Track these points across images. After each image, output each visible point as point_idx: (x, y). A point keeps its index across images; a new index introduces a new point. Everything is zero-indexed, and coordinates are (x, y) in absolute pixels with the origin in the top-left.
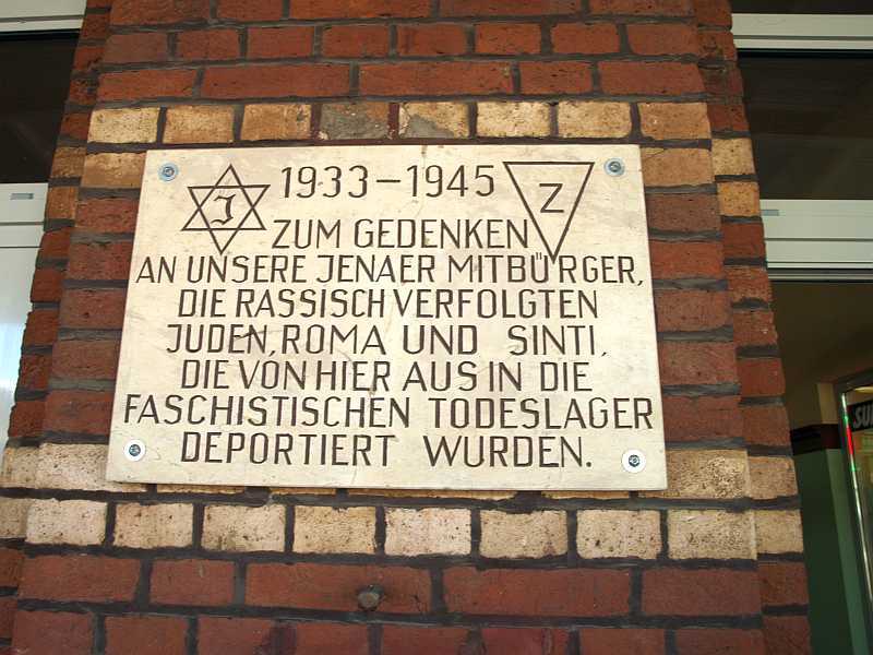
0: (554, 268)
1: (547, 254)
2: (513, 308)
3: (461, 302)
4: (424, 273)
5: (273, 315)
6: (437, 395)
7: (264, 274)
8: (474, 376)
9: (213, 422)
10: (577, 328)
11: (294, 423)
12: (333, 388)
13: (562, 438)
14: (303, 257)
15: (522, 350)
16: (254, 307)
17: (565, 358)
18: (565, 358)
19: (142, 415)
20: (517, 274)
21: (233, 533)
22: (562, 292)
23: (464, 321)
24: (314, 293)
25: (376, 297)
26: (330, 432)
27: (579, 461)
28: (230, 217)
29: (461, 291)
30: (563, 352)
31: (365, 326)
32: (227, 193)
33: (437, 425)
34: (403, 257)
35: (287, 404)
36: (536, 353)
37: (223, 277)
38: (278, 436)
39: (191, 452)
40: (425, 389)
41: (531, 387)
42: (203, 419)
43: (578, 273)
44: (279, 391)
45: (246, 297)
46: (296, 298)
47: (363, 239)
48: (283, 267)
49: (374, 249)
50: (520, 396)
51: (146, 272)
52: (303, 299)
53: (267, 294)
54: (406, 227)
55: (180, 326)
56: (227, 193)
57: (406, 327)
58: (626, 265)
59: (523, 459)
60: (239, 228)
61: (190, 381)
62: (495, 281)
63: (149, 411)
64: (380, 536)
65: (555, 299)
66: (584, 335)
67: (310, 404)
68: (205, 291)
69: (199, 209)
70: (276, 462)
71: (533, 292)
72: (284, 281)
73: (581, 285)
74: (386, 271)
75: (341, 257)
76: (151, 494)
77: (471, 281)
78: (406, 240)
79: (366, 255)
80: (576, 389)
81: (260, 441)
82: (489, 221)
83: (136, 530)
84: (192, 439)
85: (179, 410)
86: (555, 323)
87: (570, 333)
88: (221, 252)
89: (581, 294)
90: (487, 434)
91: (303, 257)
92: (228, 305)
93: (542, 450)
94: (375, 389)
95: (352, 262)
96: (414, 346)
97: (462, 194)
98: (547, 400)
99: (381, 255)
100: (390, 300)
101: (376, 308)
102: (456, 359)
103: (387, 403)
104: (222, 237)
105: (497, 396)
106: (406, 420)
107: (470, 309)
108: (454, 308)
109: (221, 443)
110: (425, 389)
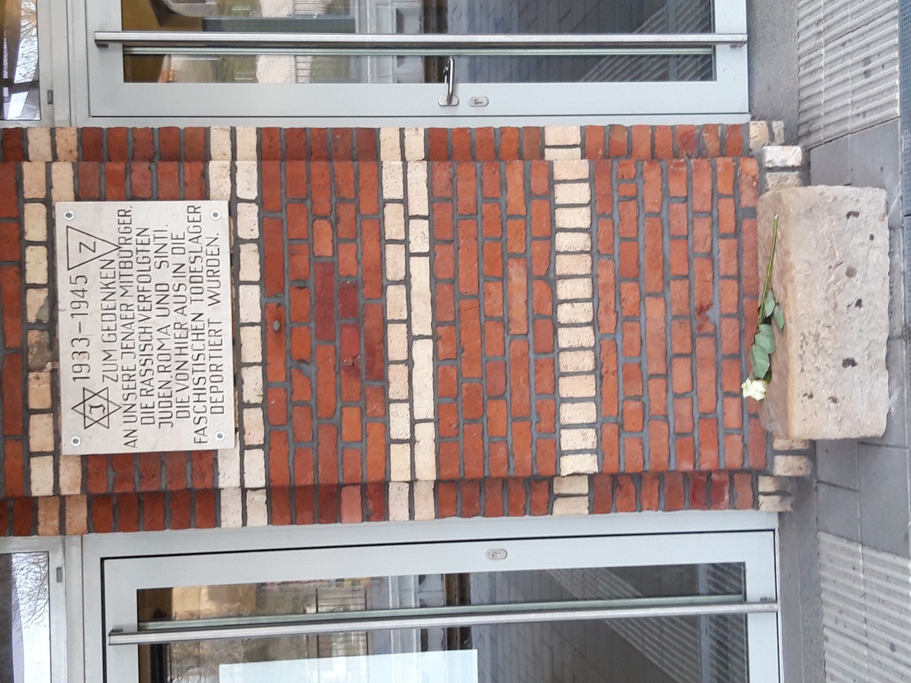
2: (146, 267)
6: (189, 301)
21: (255, 390)
23: (153, 290)
25: (142, 330)
32: (88, 408)
35: (196, 368)
39: (220, 410)
41: (183, 259)
43: (127, 236)
44: (189, 372)
45: (144, 392)
46: (144, 368)
47: (112, 338)
50: (188, 264)
51: (132, 444)
54: (105, 318)
56: (88, 408)
58: (122, 213)
59: (216, 263)
63: (201, 432)
64: (252, 324)
65: (140, 247)
66: (158, 234)
67: (195, 358)
74: (129, 326)
76: (240, 429)
81: (213, 379)
83: (256, 433)
84: (214, 410)
86: (153, 248)
90: (205, 278)
92: (148, 401)
95: (125, 343)
96: (165, 312)
99: (120, 329)
100: (142, 324)
101: (147, 330)
102: (172, 293)
104: (112, 408)
105: (189, 275)
107: (147, 286)
108: (146, 294)
109: (215, 396)
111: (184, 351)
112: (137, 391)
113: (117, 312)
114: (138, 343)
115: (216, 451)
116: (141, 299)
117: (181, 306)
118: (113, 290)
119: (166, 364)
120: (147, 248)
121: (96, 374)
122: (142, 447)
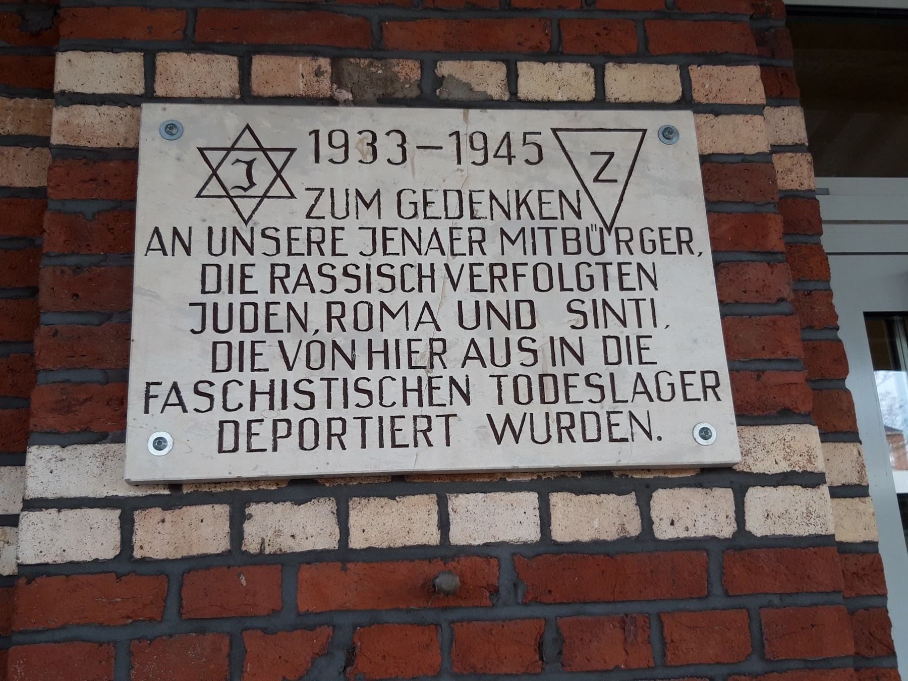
0: (610, 241)
1: (602, 226)
2: (570, 282)
3: (516, 276)
4: (476, 246)
5: (313, 291)
7: (300, 246)
8: (534, 352)
9: (253, 408)
10: (637, 301)
11: (346, 406)
12: (387, 367)
13: (630, 412)
14: (342, 229)
15: (582, 324)
16: (290, 283)
17: (626, 332)
18: (626, 332)
19: (166, 404)
20: (572, 246)
21: (278, 533)
22: (620, 265)
23: (519, 296)
24: (357, 267)
25: (426, 271)
26: (387, 414)
27: (649, 435)
28: (252, 184)
29: (515, 266)
30: (625, 326)
31: (416, 302)
32: (248, 156)
33: (500, 402)
34: (451, 229)
35: (337, 386)
36: (597, 326)
37: (251, 251)
38: (329, 420)
39: (229, 444)
40: (484, 365)
41: (594, 361)
42: (241, 405)
43: (635, 245)
44: (327, 372)
45: (280, 272)
46: (338, 273)
47: (408, 210)
48: (320, 240)
49: (420, 221)
50: (584, 371)
51: (156, 244)
52: (346, 273)
53: (304, 269)
54: (453, 198)
55: (204, 305)
56: (248, 156)
57: (460, 303)
58: (685, 236)
59: (592, 434)
60: (265, 196)
61: (222, 363)
62: (549, 253)
63: (174, 399)
64: (444, 525)
65: (613, 271)
66: (645, 307)
67: (362, 385)
68: (231, 266)
69: (215, 173)
70: (329, 448)
71: (589, 265)
72: (322, 253)
73: (638, 257)
74: (435, 244)
75: (385, 229)
76: (177, 494)
77: (525, 253)
78: (454, 211)
79: (411, 227)
80: (641, 362)
81: (309, 427)
82: (540, 192)
83: (158, 538)
84: (229, 428)
85: (211, 397)
86: (614, 296)
87: (631, 307)
88: (246, 222)
89: (640, 266)
91: (342, 229)
92: (259, 280)
93: (610, 426)
94: (432, 366)
96: (470, 321)
97: (510, 163)
98: (612, 375)
100: (440, 273)
101: (427, 282)
102: (515, 335)
103: (446, 380)
104: (246, 206)
105: (559, 371)
106: (466, 398)
107: (526, 283)
108: (509, 281)
109: (264, 432)
110: (484, 365)
111: (378, 360)
112: (283, 258)
113: (466, 222)
114: (398, 262)
115: (121, 438)
116: (498, 271)
117: (486, 353)
118: (513, 214)
119: (348, 320)
120: (614, 284)
121: (326, 175)
122: (146, 267)
